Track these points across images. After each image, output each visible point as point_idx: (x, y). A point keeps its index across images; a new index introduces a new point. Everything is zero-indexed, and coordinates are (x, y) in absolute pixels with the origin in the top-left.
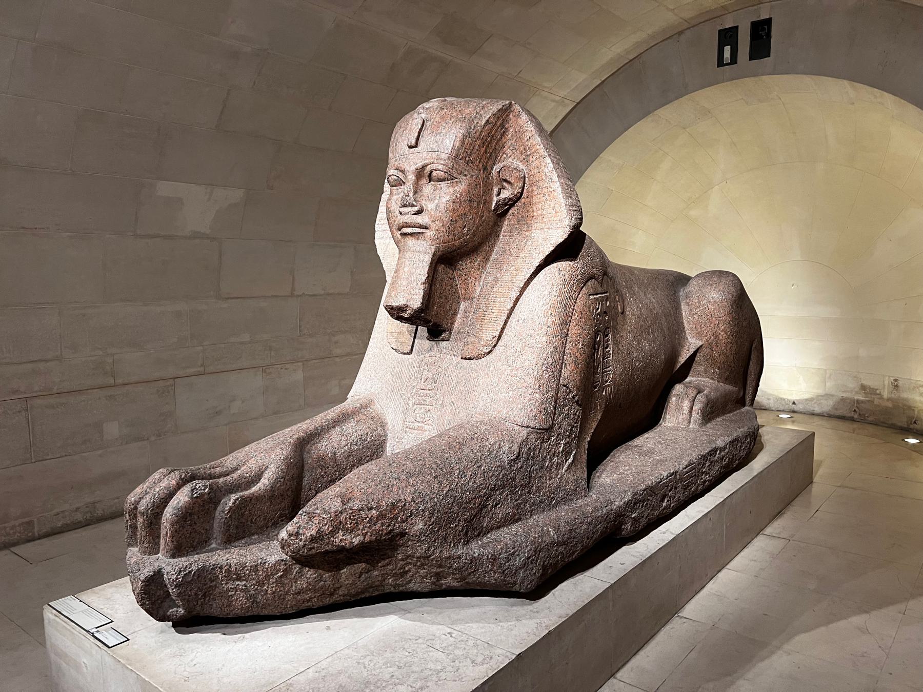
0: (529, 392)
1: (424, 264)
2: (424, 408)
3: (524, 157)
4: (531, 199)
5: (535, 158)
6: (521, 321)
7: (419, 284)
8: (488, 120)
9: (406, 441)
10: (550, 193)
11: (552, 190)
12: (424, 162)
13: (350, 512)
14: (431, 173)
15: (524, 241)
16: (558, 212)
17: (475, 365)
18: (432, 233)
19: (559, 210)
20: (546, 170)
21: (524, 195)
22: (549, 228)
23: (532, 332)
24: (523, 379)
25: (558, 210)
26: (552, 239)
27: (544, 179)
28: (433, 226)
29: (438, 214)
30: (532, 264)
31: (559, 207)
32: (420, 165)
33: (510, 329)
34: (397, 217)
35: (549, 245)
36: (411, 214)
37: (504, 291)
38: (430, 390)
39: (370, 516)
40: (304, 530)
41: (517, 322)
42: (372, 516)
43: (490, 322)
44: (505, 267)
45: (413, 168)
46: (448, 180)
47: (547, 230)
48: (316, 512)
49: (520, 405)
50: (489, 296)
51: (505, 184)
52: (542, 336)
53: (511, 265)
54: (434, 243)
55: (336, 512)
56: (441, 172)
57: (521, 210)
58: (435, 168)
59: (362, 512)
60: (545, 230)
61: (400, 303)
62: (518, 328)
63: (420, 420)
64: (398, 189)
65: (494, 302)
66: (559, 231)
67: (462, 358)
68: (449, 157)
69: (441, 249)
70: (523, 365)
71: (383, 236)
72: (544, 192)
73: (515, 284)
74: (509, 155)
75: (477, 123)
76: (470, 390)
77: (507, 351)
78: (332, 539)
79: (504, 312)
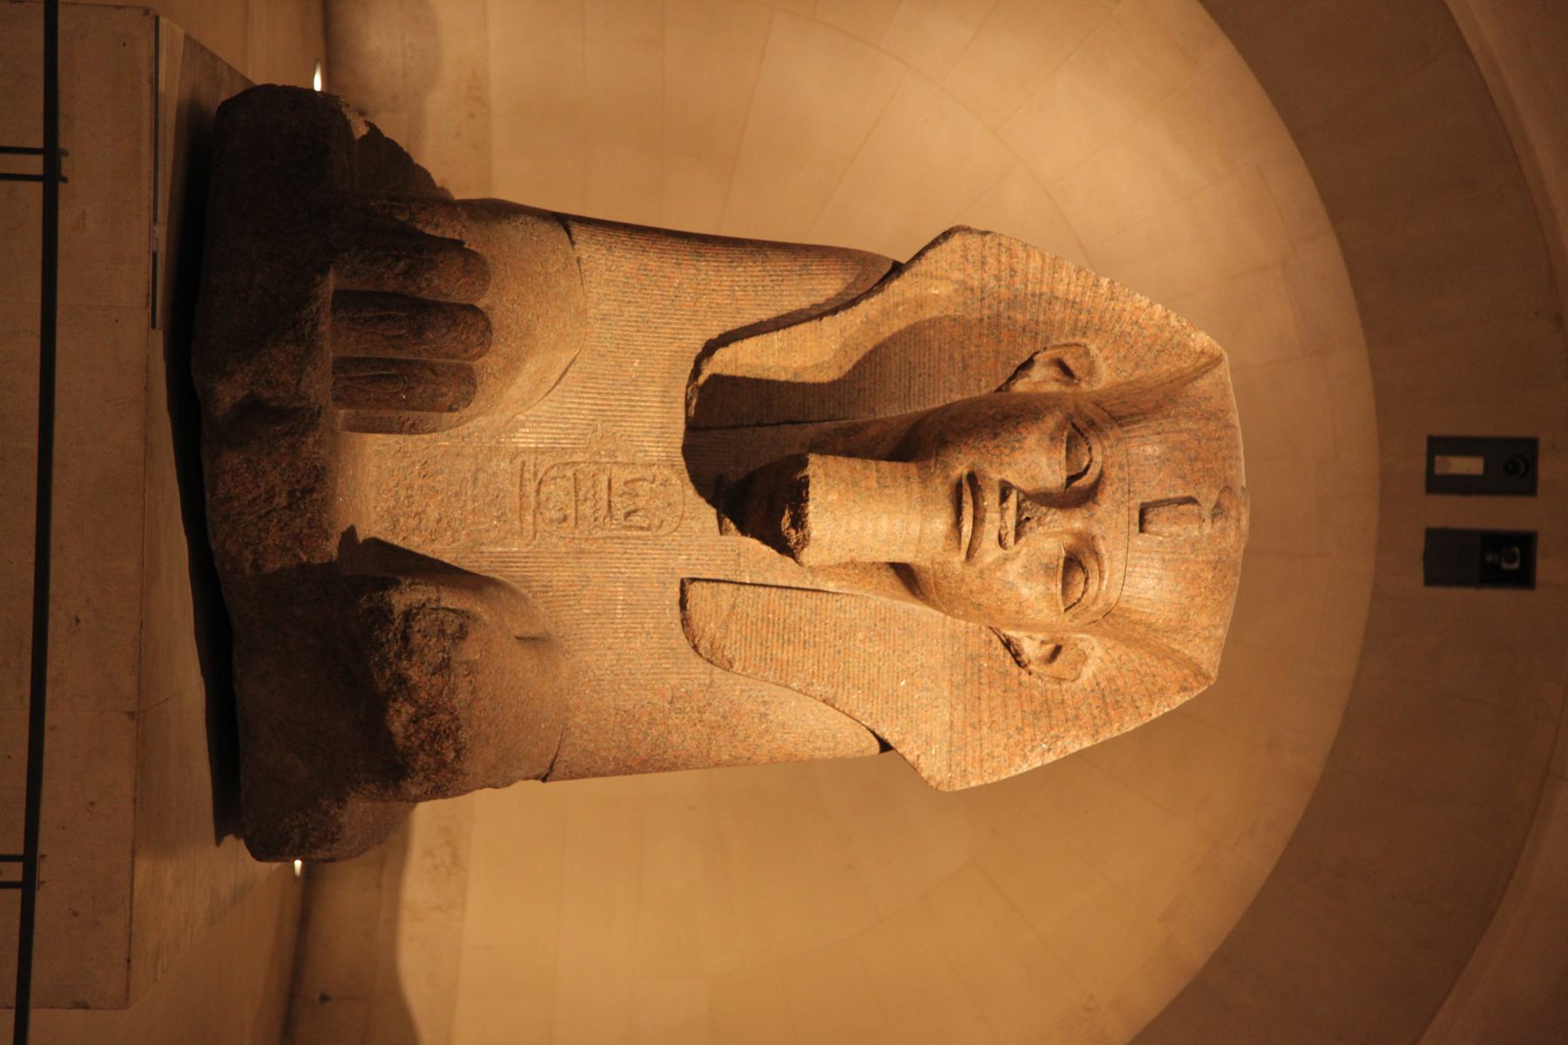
0: (619, 755)
1: (894, 554)
2: (570, 500)
3: (1102, 685)
4: (1015, 694)
5: (1096, 712)
6: (762, 709)
7: (853, 554)
8: (1179, 651)
9: (495, 468)
10: (1021, 746)
11: (1028, 754)
12: (1106, 557)
13: (453, 727)
14: (1083, 569)
15: (929, 683)
16: (981, 767)
17: (669, 621)
18: (958, 566)
19: (985, 768)
20: (1068, 740)
21: (1025, 677)
22: (951, 745)
23: (741, 736)
24: (646, 738)
25: (986, 765)
26: (929, 757)
27: (1052, 733)
28: (972, 572)
29: (996, 586)
30: (881, 721)
31: (991, 771)
32: (1102, 547)
33: (747, 688)
34: (1000, 472)
35: (916, 753)
36: (1001, 528)
37: (826, 664)
38: (610, 507)
39: (444, 751)
40: (419, 664)
41: (760, 700)
42: (443, 754)
43: (761, 644)
44: (877, 649)
45: (1096, 530)
46: (1063, 600)
47: (948, 738)
48: (452, 676)
49: (592, 745)
50: (818, 623)
51: (1049, 647)
52: (733, 753)
53: (881, 663)
54: (936, 566)
55: (453, 708)
56: (1079, 595)
57: (996, 665)
58: (1090, 581)
59: (451, 742)
60: (948, 734)
61: (813, 525)
62: (749, 707)
63: (543, 497)
64: (1060, 464)
65: (805, 643)
66: (944, 769)
67: (683, 583)
68: (1111, 604)
69: (923, 575)
70: (674, 731)
71: (970, 259)
72: (1027, 729)
73: (840, 691)
74: (1111, 651)
75: (1175, 640)
76: (617, 621)
77: (702, 691)
78: (401, 699)
79: (784, 676)
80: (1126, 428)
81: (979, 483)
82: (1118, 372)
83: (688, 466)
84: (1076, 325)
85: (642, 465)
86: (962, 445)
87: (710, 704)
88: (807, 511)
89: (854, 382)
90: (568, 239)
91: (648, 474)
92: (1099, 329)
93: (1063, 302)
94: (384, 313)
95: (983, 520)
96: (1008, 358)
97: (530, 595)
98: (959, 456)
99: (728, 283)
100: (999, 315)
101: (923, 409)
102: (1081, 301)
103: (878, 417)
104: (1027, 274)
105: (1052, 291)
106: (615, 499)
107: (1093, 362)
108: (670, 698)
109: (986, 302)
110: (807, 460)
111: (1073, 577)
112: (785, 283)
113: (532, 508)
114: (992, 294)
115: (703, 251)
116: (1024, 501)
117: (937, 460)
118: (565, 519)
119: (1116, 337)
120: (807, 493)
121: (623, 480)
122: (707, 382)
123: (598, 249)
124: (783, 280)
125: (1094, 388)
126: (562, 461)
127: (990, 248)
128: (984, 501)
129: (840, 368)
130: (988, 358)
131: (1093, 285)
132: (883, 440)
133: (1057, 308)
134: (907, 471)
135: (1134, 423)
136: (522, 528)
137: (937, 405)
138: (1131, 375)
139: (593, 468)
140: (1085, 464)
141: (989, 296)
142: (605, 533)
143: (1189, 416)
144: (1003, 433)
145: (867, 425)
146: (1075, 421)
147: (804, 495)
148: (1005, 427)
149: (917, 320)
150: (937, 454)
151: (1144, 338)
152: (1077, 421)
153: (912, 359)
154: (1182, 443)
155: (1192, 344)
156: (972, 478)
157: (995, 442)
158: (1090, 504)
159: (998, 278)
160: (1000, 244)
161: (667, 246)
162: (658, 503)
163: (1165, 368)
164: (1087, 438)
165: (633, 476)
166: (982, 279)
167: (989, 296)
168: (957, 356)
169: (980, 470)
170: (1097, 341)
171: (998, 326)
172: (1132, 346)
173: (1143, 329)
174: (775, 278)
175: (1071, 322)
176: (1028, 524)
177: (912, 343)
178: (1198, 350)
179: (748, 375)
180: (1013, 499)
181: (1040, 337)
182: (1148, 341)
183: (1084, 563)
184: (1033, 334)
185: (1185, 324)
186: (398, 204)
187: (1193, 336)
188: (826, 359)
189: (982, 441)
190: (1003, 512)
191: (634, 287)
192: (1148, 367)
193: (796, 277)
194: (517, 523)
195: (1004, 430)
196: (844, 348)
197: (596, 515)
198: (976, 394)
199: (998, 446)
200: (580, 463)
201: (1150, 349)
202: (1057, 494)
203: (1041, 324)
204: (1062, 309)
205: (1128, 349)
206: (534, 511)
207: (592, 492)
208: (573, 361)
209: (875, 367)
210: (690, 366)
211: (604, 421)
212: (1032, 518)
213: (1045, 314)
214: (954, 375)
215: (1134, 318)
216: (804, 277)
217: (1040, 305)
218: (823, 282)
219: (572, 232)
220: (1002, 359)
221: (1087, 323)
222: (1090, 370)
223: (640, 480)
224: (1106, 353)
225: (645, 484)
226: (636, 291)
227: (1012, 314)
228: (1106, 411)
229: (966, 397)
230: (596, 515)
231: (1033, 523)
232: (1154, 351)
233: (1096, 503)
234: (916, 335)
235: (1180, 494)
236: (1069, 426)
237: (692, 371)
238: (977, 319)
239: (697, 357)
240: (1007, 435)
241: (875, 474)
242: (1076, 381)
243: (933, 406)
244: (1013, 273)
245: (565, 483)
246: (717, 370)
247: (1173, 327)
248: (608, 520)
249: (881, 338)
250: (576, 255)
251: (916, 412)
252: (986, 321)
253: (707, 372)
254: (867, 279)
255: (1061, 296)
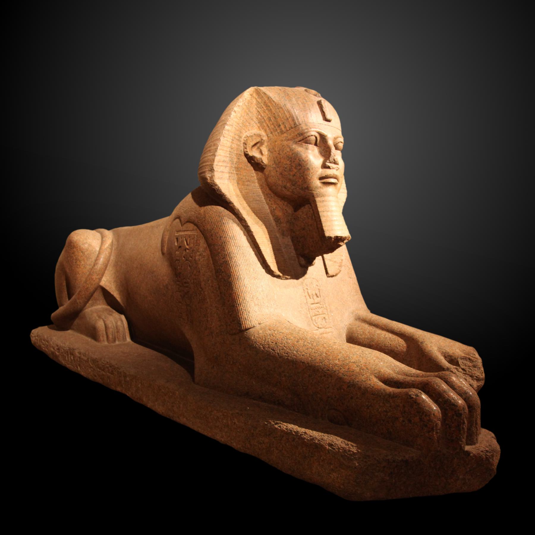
14: (339, 143)
67: (327, 277)
71: (222, 177)
80: (301, 123)
81: (324, 176)
82: (253, 126)
83: (301, 277)
84: (239, 140)
85: (305, 293)
86: (310, 181)
87: (348, 266)
88: (344, 237)
89: (264, 220)
90: (251, 329)
91: (306, 291)
92: (240, 132)
93: (232, 144)
94: (474, 423)
95: (336, 175)
96: (246, 166)
97: (346, 326)
98: (314, 182)
99: (245, 267)
100: (235, 168)
101: (263, 196)
102: (232, 137)
103: (269, 212)
104: (225, 156)
105: (229, 147)
106: (316, 301)
107: (255, 134)
108: (350, 279)
109: (232, 172)
110: (328, 236)
111: (340, 147)
112: (239, 245)
113: (325, 329)
114: (230, 169)
115: (236, 277)
116: (330, 161)
117: (314, 191)
118: (324, 318)
119: (243, 126)
120: (340, 237)
121: (310, 299)
122: (281, 273)
123: (251, 317)
124: (239, 246)
125: (265, 135)
126: (311, 321)
127: (218, 169)
128: (331, 175)
129: (262, 225)
130: (246, 173)
131: (228, 132)
132: (286, 210)
133: (233, 146)
134: (320, 202)
135: (298, 119)
136: (331, 332)
137: (260, 191)
138: (255, 122)
139: (311, 311)
140: (315, 138)
141: (231, 171)
142: (324, 304)
143: (290, 100)
144: (307, 166)
145: (273, 216)
146: (298, 141)
147: (340, 238)
148: (305, 165)
149: (242, 197)
150: (311, 190)
151: (244, 115)
152: (297, 140)
153: (252, 199)
154: (302, 103)
155: (248, 99)
156: (321, 178)
157: (310, 169)
158: (326, 138)
159: (226, 167)
160: (217, 165)
161: (238, 290)
162: (312, 287)
163: (254, 109)
164: (309, 136)
165: (309, 297)
166: (226, 173)
167: (231, 171)
168: (246, 183)
169: (319, 175)
170: (243, 133)
171: (238, 168)
172: (246, 120)
173: (242, 115)
174: (239, 249)
175: (237, 141)
176: (336, 160)
177: (248, 199)
178: (250, 96)
179: (274, 258)
180: (328, 164)
181: (240, 153)
182: (245, 115)
183: (337, 142)
184: (239, 156)
185: (242, 100)
186: (435, 427)
187: (246, 98)
188: (261, 230)
189: (310, 174)
190: (333, 168)
191: (258, 302)
192: (253, 115)
193: (237, 242)
194: (330, 334)
195: (306, 166)
196: (257, 223)
197: (321, 307)
198: (255, 178)
199: (312, 168)
200: (310, 315)
201: (248, 114)
202: (319, 149)
203: (237, 153)
204: (234, 144)
205: (247, 122)
206: (325, 329)
207: (316, 309)
208: (288, 321)
209: (258, 212)
210: (275, 278)
211: (298, 308)
212: (334, 158)
213: (235, 151)
214: (251, 185)
215: (239, 118)
216: (236, 239)
217: (232, 152)
218: (235, 231)
219: (249, 327)
220: (246, 168)
221: (238, 136)
222: (258, 136)
223: (308, 294)
224: (247, 130)
225: (309, 292)
226: (259, 301)
227: (235, 163)
228: (290, 129)
229: (256, 181)
230: (321, 307)
231: (335, 158)
232: (249, 112)
233: (326, 136)
234: (246, 198)
235: (317, 107)
236: (300, 143)
237: (277, 278)
238: (237, 175)
239: (272, 276)
240: (308, 165)
241: (325, 213)
242: (263, 141)
243: (261, 193)
244: (224, 161)
245: (316, 319)
246: (277, 269)
247: (243, 104)
248: (321, 303)
249: (250, 210)
250: (258, 325)
251: (264, 199)
252: (238, 173)
253: (278, 273)
254: (228, 215)
255: (230, 144)
